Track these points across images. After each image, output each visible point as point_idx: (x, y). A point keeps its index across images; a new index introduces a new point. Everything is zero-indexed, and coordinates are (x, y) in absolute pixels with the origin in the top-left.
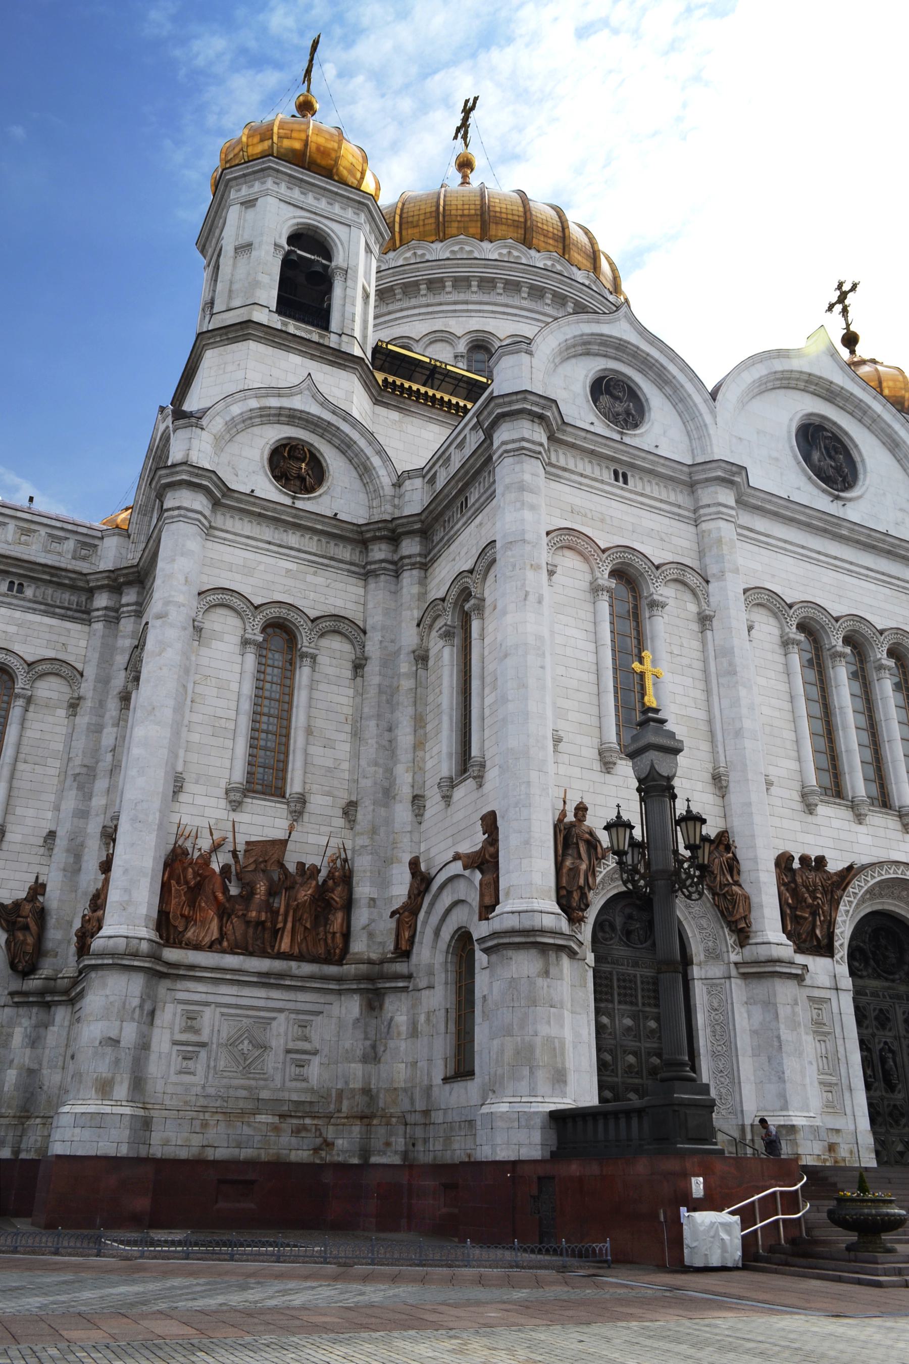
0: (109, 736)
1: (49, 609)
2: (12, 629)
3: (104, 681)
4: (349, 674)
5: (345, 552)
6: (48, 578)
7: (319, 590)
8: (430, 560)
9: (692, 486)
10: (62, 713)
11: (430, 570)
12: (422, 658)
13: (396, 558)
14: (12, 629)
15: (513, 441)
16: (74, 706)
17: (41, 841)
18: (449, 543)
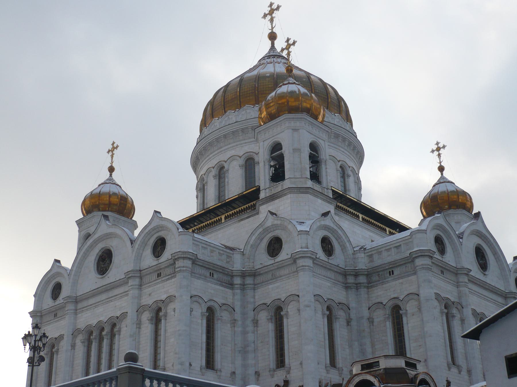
0: (251, 337)
1: (222, 283)
2: (212, 292)
3: (244, 314)
4: (345, 324)
5: (340, 278)
6: (221, 271)
7: (338, 294)
8: (371, 286)
9: (457, 274)
10: (229, 325)
11: (370, 290)
12: (371, 320)
13: (357, 282)
14: (212, 292)
15: (425, 265)
16: (234, 322)
17: (229, 375)
18: (383, 283)
